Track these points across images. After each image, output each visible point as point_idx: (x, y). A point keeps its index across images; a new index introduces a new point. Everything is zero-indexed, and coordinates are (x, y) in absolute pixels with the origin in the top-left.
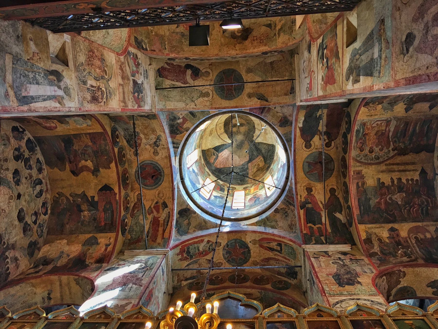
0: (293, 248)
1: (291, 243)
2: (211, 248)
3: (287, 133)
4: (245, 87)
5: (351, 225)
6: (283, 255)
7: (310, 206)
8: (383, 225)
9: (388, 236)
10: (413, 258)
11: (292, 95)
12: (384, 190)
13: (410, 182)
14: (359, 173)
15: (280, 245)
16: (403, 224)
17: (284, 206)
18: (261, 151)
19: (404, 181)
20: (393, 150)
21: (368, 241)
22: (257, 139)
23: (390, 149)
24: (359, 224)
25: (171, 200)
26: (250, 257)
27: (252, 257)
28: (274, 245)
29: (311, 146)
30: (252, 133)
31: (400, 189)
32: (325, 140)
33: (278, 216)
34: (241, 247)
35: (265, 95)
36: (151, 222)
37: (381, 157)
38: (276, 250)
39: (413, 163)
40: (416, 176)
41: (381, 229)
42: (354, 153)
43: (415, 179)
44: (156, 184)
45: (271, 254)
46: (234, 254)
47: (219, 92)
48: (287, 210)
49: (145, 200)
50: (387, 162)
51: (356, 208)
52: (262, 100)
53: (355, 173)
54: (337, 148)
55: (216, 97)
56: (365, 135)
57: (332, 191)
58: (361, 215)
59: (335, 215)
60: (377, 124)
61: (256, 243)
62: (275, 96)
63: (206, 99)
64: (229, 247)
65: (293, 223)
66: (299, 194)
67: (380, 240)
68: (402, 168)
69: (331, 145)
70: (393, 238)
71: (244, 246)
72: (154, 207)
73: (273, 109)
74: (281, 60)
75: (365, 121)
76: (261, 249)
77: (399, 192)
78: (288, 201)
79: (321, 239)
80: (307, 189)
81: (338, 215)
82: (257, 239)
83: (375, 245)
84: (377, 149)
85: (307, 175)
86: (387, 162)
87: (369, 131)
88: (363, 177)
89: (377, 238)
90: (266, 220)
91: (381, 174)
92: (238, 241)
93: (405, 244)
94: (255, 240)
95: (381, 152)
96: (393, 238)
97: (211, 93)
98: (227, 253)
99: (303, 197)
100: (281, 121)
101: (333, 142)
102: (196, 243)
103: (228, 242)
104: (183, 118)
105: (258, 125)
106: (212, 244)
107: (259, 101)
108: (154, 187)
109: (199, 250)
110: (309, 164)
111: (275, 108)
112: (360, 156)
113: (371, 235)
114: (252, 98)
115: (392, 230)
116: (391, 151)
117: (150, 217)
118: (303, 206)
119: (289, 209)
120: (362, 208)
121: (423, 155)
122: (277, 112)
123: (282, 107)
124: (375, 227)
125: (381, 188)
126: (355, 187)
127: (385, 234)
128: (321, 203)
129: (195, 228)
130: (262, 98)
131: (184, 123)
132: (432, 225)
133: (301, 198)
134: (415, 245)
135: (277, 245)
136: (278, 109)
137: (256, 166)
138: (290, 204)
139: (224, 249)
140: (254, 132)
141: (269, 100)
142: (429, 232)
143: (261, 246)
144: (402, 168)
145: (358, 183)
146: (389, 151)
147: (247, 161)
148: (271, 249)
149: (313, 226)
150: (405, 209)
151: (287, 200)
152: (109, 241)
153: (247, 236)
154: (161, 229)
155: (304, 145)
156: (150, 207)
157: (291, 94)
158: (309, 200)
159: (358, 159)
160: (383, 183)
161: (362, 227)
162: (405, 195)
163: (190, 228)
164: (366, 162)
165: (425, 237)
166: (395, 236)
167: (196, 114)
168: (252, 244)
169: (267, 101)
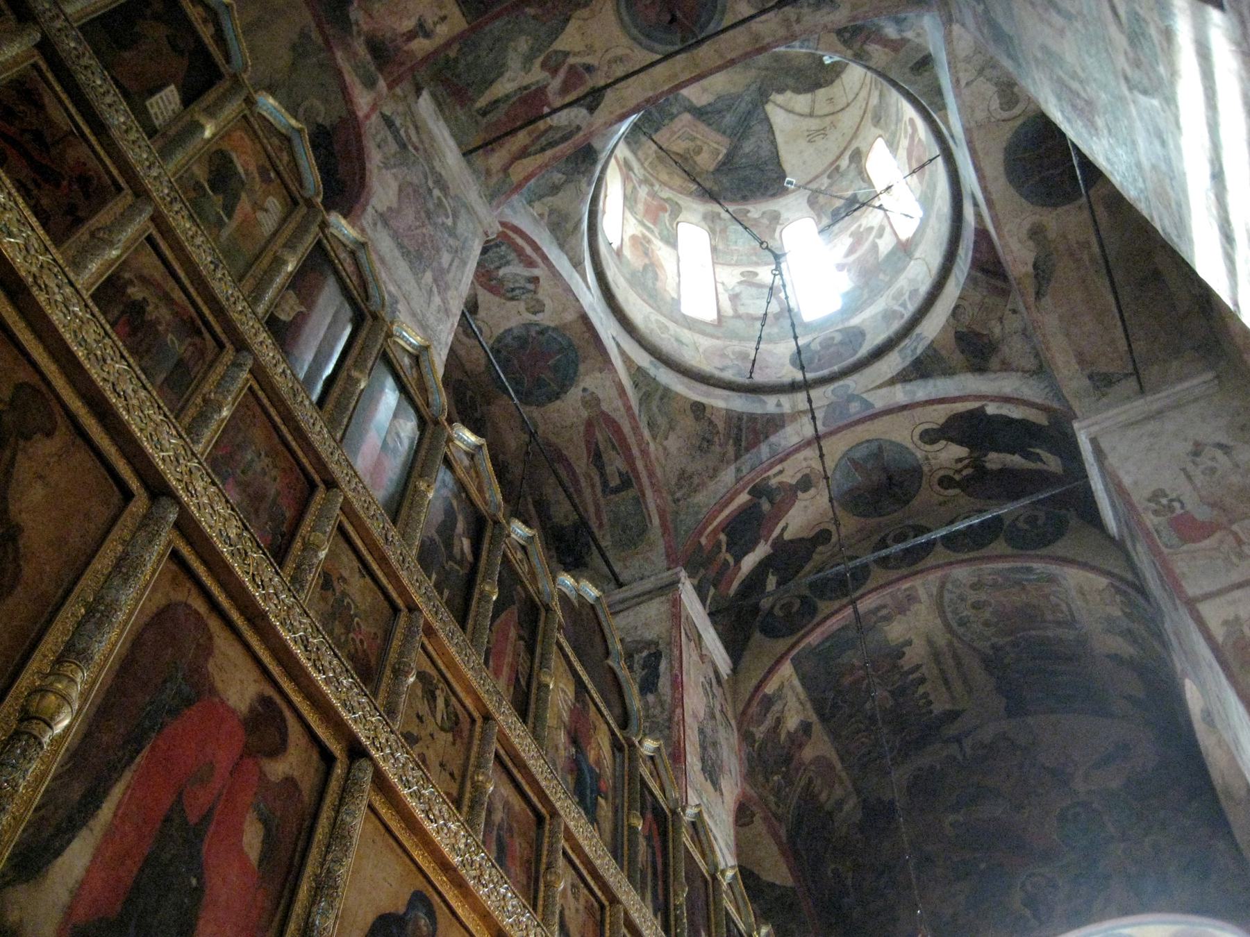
0: (643, 530)
1: (656, 521)
2: (517, 292)
4: (1060, 210)
5: (771, 631)
6: (602, 501)
7: (766, 506)
8: (809, 706)
9: (792, 730)
10: (780, 811)
11: (1088, 382)
14: (912, 598)
17: (721, 426)
19: (921, 690)
20: (993, 647)
21: (768, 702)
22: (778, 110)
23: (994, 640)
25: (619, 112)
26: (540, 405)
28: (616, 463)
29: (933, 442)
30: (790, 82)
31: (899, 693)
32: (959, 471)
33: (687, 423)
34: (555, 369)
36: (526, 88)
38: (603, 475)
39: (970, 692)
40: (938, 708)
41: (800, 707)
42: (962, 573)
43: (932, 707)
44: (648, 36)
45: (581, 463)
47: (1026, 133)
48: (716, 439)
49: (581, 22)
50: (957, 644)
51: (823, 633)
52: (1036, 276)
53: (908, 593)
55: (1005, 133)
57: (822, 537)
58: (813, 651)
59: (770, 577)
60: (1058, 605)
62: (1061, 318)
63: (995, 104)
65: (696, 480)
66: (785, 464)
67: (779, 721)
68: (953, 674)
69: (946, 489)
70: (793, 742)
71: (565, 379)
72: (572, 67)
74: (1174, 307)
75: (1064, 582)
76: (582, 428)
77: (892, 693)
78: (741, 430)
79: (708, 591)
80: (806, 476)
81: (771, 582)
82: (604, 407)
83: (767, 722)
84: (987, 614)
86: (957, 644)
88: (902, 610)
89: (778, 715)
90: (659, 393)
94: (598, 400)
95: (980, 626)
97: (1017, 111)
98: (519, 338)
100: (978, 335)
101: (957, 491)
102: (520, 252)
103: (555, 329)
104: (904, 41)
106: (529, 291)
107: (1030, 269)
108: (635, 32)
109: (499, 268)
110: (878, 454)
111: (1014, 311)
112: (958, 587)
113: (780, 697)
114: (1031, 243)
115: (806, 728)
117: (537, 75)
118: (757, 492)
119: (720, 445)
122: (1001, 320)
123: (1025, 334)
124: (797, 695)
127: (792, 723)
128: (784, 529)
129: (551, 212)
130: (1042, 273)
131: (886, 42)
133: (775, 475)
134: (799, 789)
135: (620, 474)
136: (1013, 323)
138: (738, 441)
139: (527, 326)
140: (797, 91)
141: (1043, 301)
143: (589, 424)
144: (953, 674)
145: (884, 606)
146: (989, 639)
147: (695, 101)
148: (597, 458)
149: (724, 548)
151: (744, 426)
152: (435, 24)
153: (598, 375)
154: (522, 138)
155: (927, 426)
156: (566, 54)
157: (1090, 377)
158: (778, 498)
159: (949, 586)
161: (787, 669)
163: (545, 200)
165: (821, 792)
168: (583, 397)
169: (1039, 295)
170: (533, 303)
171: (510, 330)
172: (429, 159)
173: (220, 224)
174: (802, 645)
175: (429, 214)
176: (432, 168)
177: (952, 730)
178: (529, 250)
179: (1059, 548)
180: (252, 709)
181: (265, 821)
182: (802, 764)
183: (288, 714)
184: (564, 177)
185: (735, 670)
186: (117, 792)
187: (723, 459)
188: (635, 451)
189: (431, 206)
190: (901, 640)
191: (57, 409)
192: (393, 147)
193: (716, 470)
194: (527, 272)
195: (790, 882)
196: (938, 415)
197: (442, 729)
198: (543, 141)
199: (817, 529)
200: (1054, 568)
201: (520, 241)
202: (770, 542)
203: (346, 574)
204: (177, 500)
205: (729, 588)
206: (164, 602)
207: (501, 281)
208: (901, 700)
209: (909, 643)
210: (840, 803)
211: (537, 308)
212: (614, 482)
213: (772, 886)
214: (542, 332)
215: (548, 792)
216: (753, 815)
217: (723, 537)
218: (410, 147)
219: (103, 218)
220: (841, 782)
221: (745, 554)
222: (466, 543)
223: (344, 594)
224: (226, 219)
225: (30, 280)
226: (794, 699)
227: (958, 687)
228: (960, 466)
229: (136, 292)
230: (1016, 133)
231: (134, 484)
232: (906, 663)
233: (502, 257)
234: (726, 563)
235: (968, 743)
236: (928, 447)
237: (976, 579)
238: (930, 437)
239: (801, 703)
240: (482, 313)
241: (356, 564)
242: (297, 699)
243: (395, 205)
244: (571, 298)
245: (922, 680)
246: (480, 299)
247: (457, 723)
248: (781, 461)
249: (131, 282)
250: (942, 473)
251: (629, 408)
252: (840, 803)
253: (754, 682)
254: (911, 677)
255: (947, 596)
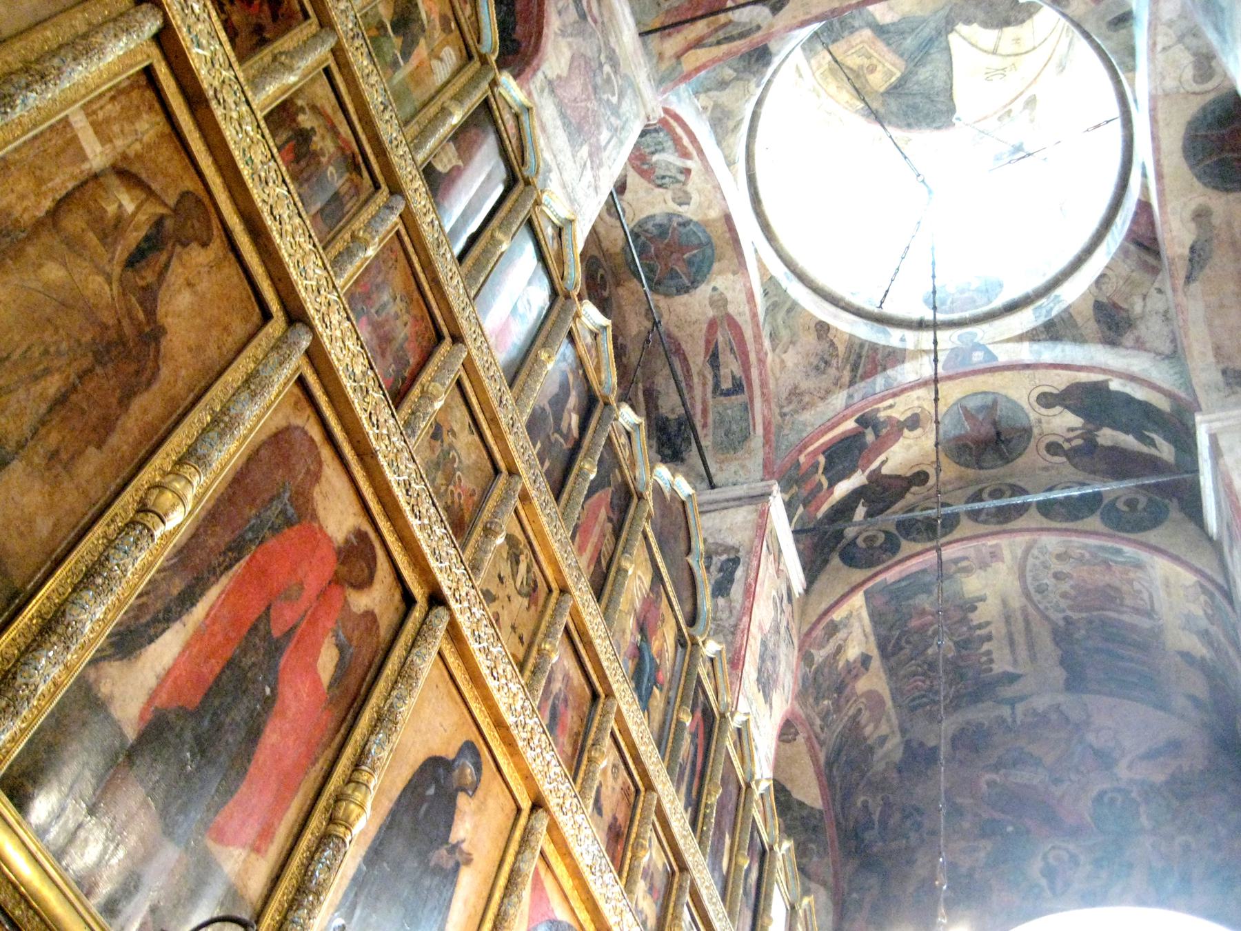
0: (746, 437)
1: (760, 430)
2: (667, 180)
3: (1075, 325)
5: (850, 559)
6: (711, 402)
7: (870, 437)
8: (872, 639)
10: (822, 736)
12: (957, 615)
13: (984, 659)
14: (995, 555)
15: (738, 388)
16: (882, 674)
17: (841, 349)
18: (919, 63)
19: (986, 647)
20: (1066, 619)
23: (1069, 613)
24: (866, 593)
25: (802, 17)
26: (667, 295)
27: (669, 301)
28: (731, 366)
29: (1048, 406)
31: (963, 645)
32: (1069, 440)
33: (809, 340)
34: (690, 263)
35: (1207, 271)
37: (1044, 598)
38: (716, 376)
39: (1033, 658)
40: (997, 668)
42: (1051, 542)
43: (994, 666)
45: (698, 360)
46: (661, 246)
48: (834, 362)
50: (1031, 609)
52: (1191, 260)
54: (1046, 469)
55: (1192, 108)
56: (1106, 564)
57: (920, 478)
58: (886, 588)
60: (1140, 592)
61: (718, 307)
63: (1189, 73)
64: (681, 229)
65: (806, 399)
66: (897, 399)
67: (839, 649)
68: (1020, 639)
70: (849, 672)
71: (698, 273)
73: (1157, 285)
76: (705, 327)
77: (956, 644)
78: (860, 356)
81: (860, 512)
82: (731, 309)
84: (1065, 586)
85: (955, 408)
86: (1031, 609)
87: (1118, 574)
88: (984, 565)
91: (998, 602)
92: (709, 251)
93: (843, 700)
94: (725, 302)
96: (849, 672)
98: (661, 226)
99: (889, 412)
100: (1115, 305)
102: (677, 141)
103: (696, 224)
105: (1017, 40)
106: (678, 181)
107: (1186, 252)
109: (653, 153)
111: (1160, 291)
113: (845, 626)
114: (1192, 226)
115: (865, 660)
116: (1061, 615)
118: (864, 422)
119: (837, 368)
120: (903, 584)
121: (1059, 674)
122: (1145, 297)
123: (1166, 317)
125: (961, 607)
126: (953, 556)
127: (853, 652)
128: (883, 463)
129: (716, 106)
130: (1198, 257)
132: (891, 727)
133: (885, 409)
135: (734, 377)
137: (866, 62)
138: (855, 368)
139: (670, 216)
140: (985, 25)
142: (876, 727)
143: (712, 325)
144: (1020, 639)
148: (714, 358)
149: (821, 470)
150: (919, 665)
151: (864, 353)
153: (730, 276)
154: (701, 27)
155: (1047, 389)
157: (1224, 372)
158: (884, 431)
159: (1035, 552)
160: (974, 609)
161: (858, 600)
162: (950, 656)
163: (711, 94)
164: (1028, 568)
165: (866, 726)
166: (854, 672)
167: (1123, 32)
168: (711, 298)
169: (1189, 279)
170: (681, 194)
171: (652, 217)
172: (605, 33)
173: (395, 65)
174: (878, 579)
175: (595, 88)
176: (607, 44)
177: (1008, 692)
178: (686, 141)
179: (1152, 536)
180: (347, 541)
181: (341, 648)
182: (853, 693)
183: (380, 553)
184: (735, 74)
185: (807, 591)
186: (213, 594)
187: (837, 383)
188: (753, 357)
189: (599, 80)
190: (977, 594)
191: (215, 222)
192: (572, 15)
193: (828, 392)
194: (680, 162)
195: (818, 804)
196: (1059, 381)
197: (519, 593)
198: (721, 35)
199: (916, 470)
200: (1144, 555)
201: (679, 131)
202: (867, 472)
203: (456, 428)
204: (312, 328)
205: (818, 509)
206: (283, 423)
207: (653, 167)
208: (964, 652)
209: (982, 599)
210: (883, 740)
211: (684, 200)
212: (726, 385)
213: (801, 804)
214: (685, 224)
215: (607, 672)
216: (797, 733)
217: (822, 460)
218: (589, 19)
219: (287, 43)
220: (889, 720)
221: (840, 480)
222: (575, 419)
223: (451, 447)
224: (401, 62)
225: (211, 93)
226: (860, 630)
227: (1023, 653)
228: (1071, 435)
229: (306, 120)
230: (1204, 109)
231: (274, 306)
232: (976, 618)
233: (660, 143)
234: (820, 484)
235: (1020, 708)
236: (1043, 411)
237: (1063, 549)
238: (1047, 400)
239: (865, 635)
240: (628, 195)
241: (468, 420)
242: (390, 539)
243: (565, 74)
244: (719, 196)
245: (989, 638)
246: (629, 181)
247: (535, 588)
248: (894, 395)
249: (302, 110)
250: (1052, 439)
251: (754, 315)
252: (883, 740)
253: (824, 606)
254: (978, 632)
255: (1031, 561)
